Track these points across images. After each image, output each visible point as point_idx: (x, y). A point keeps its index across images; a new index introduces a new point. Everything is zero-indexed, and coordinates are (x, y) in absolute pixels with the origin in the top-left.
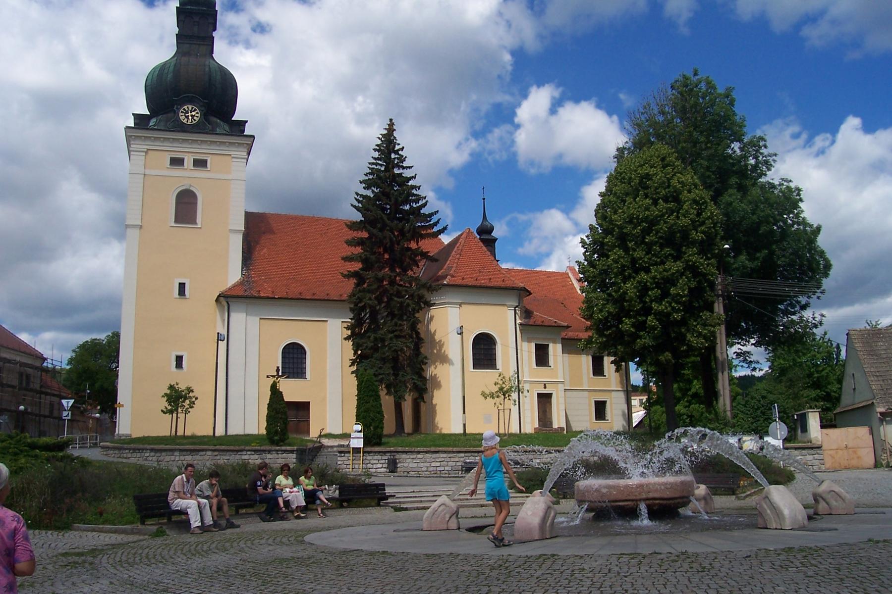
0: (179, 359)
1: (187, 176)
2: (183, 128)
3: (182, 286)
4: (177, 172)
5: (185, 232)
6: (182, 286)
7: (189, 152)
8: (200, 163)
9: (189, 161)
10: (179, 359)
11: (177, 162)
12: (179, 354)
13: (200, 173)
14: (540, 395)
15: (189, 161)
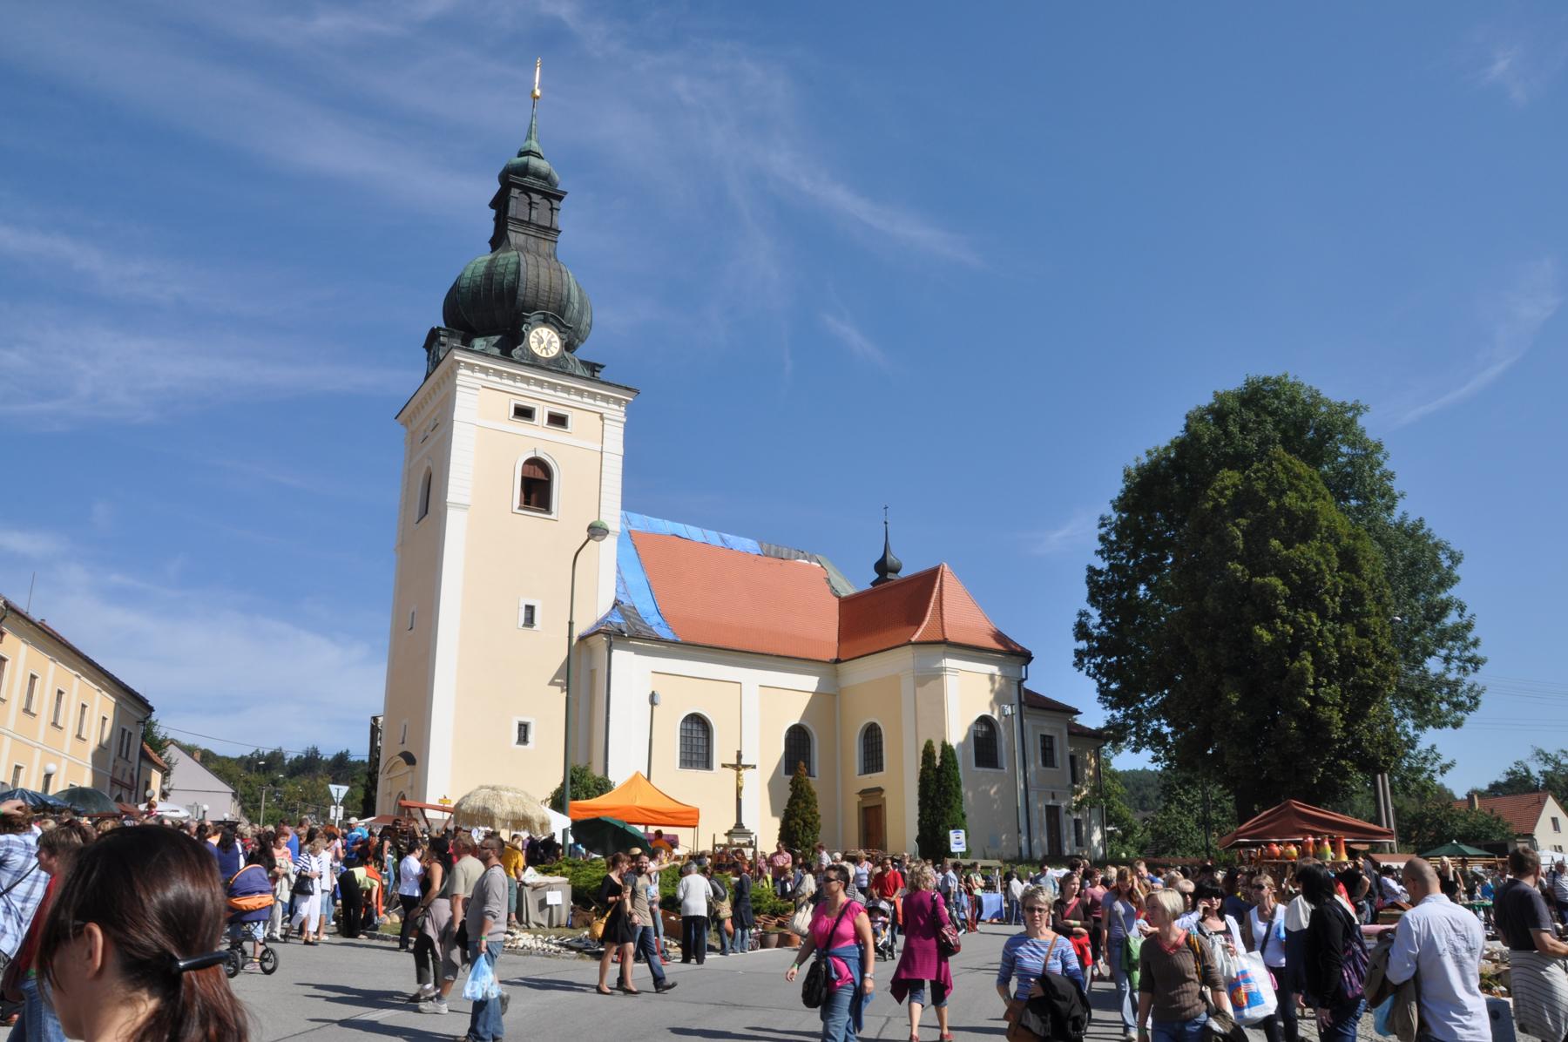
0: (524, 729)
1: (537, 439)
2: (535, 362)
3: (530, 609)
4: (522, 426)
5: (534, 519)
6: (530, 609)
7: (544, 400)
8: (558, 420)
9: (541, 416)
10: (524, 729)
11: (524, 413)
12: (524, 720)
13: (555, 433)
14: (1048, 807)
15: (541, 416)
